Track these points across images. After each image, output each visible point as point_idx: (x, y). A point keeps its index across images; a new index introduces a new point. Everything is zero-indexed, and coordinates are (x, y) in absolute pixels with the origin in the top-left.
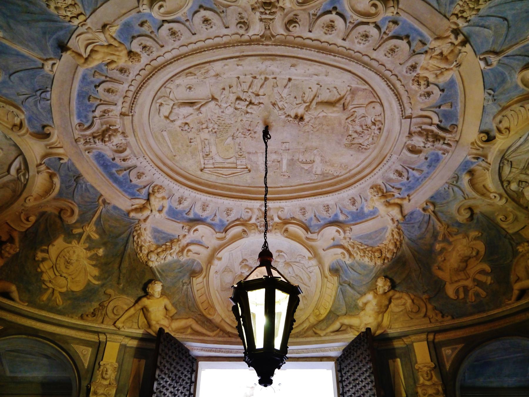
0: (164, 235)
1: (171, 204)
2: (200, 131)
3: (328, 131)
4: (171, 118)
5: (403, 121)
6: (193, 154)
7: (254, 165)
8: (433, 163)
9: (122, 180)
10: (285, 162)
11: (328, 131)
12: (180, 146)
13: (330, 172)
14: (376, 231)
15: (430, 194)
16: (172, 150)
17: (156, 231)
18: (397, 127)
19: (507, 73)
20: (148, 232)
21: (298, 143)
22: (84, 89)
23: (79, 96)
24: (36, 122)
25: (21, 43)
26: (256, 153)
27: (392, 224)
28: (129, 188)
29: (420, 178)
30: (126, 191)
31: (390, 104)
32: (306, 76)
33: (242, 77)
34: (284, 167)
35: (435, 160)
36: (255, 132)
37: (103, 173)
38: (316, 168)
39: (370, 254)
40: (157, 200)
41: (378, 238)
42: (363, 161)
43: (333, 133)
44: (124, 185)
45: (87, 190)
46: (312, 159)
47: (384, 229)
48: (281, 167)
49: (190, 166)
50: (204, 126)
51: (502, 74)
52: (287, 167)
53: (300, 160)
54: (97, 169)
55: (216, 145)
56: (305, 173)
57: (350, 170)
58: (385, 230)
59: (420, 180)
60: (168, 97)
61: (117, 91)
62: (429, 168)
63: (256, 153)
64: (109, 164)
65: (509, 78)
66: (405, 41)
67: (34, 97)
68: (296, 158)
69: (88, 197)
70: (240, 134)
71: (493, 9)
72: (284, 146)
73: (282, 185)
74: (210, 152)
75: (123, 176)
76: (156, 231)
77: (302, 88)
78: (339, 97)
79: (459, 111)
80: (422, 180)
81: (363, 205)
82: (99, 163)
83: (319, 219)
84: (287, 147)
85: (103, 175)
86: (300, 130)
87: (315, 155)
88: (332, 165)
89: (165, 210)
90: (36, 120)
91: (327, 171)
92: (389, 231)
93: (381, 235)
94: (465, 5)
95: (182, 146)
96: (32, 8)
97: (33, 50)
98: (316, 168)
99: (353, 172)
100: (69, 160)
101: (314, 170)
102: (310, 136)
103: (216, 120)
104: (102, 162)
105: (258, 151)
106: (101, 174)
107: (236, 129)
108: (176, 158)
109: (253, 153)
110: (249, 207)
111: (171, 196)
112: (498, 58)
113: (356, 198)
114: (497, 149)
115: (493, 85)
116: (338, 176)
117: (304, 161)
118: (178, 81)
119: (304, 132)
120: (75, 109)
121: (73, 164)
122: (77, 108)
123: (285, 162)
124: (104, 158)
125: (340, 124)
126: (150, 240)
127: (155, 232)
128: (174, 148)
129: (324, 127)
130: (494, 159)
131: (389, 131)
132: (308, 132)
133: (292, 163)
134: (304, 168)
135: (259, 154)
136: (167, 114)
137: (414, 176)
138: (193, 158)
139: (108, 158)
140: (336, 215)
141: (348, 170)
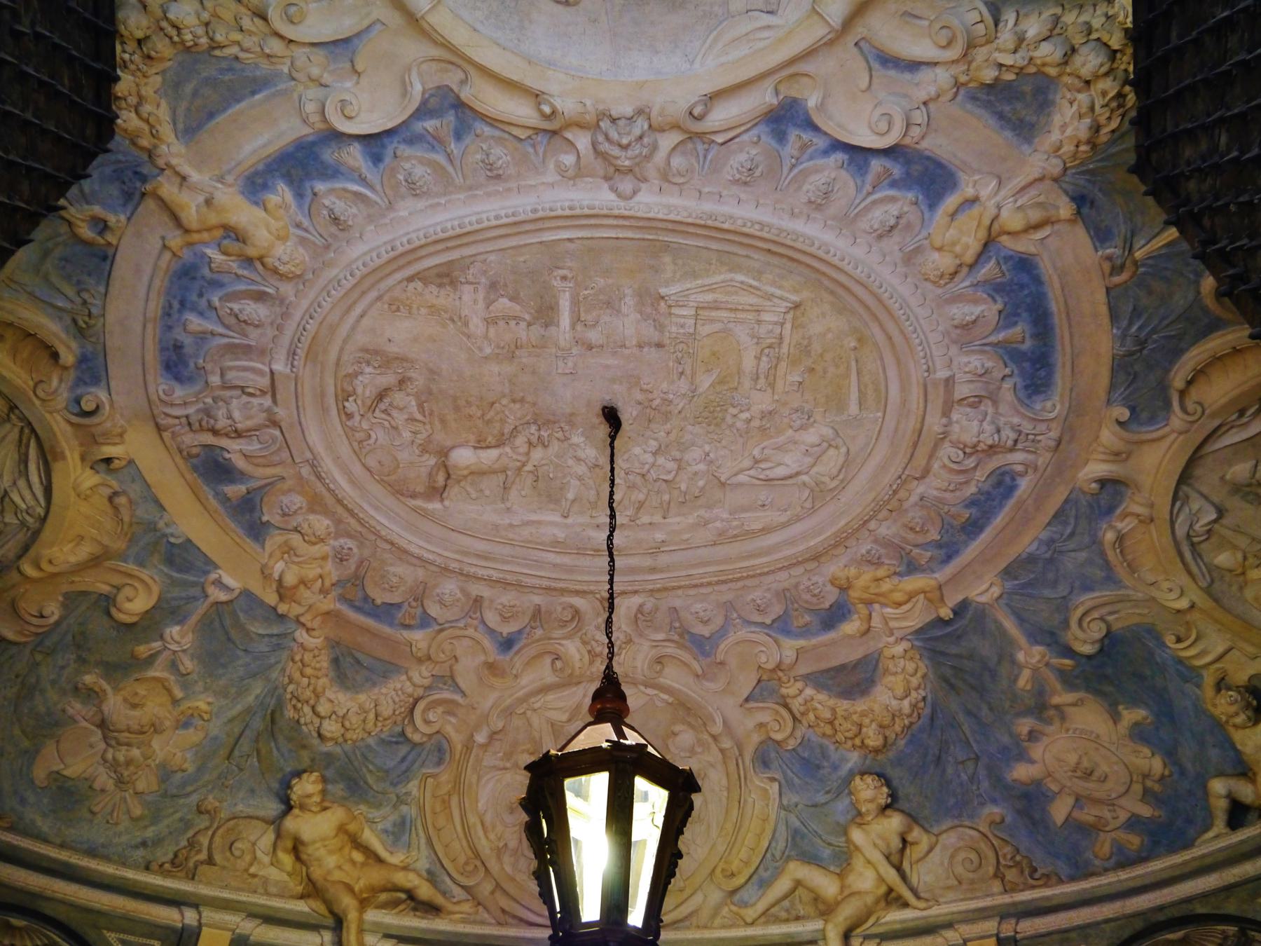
0: (1007, 108)
1: (927, 215)
2: (770, 413)
3: (467, 402)
4: (825, 445)
5: (309, 455)
6: (806, 350)
7: (649, 310)
8: (174, 358)
9: (1025, 315)
10: (565, 320)
11: (467, 402)
12: (832, 370)
13: (433, 288)
14: (211, 115)
15: (122, 268)
16: (853, 363)
17: (1025, 130)
18: (314, 437)
19: (175, 575)
20: (1055, 136)
21: (534, 372)
22: (963, 537)
23: (981, 529)
24: (1102, 502)
25: (1003, 633)
26: (640, 346)
27: (174, 161)
28: (1022, 287)
29: (180, 311)
30: (1038, 281)
31: (353, 481)
32: (533, 522)
33: (657, 518)
34: (565, 304)
35: (176, 366)
36: (640, 404)
37: (1059, 348)
38: (475, 301)
39: (188, 37)
40: (958, 249)
41: (189, 88)
42: (353, 328)
43: (455, 399)
44: (1028, 300)
45: (1136, 313)
46: (492, 331)
47: (189, 132)
48: (575, 303)
49: (824, 315)
50: (756, 423)
51: (180, 571)
52: (557, 304)
53: (523, 325)
54: (1064, 366)
55: (740, 372)
56: (506, 285)
57: (379, 298)
58: (181, 126)
59: (176, 305)
60: (812, 491)
61: (906, 526)
62: (176, 340)
63: (640, 346)
64: (1027, 365)
65: (166, 570)
66: (379, 602)
67: (1064, 548)
68: (537, 330)
69: (1150, 293)
70: (675, 402)
71: (273, 660)
72: (570, 364)
73: (569, 244)
74: (758, 358)
75: (1015, 324)
76: (1025, 130)
77: (539, 495)
78: (462, 484)
79: (205, 488)
80: (171, 306)
81: (300, 206)
82: (1050, 374)
83: (431, 139)
84: (561, 364)
85: (1063, 345)
86: (534, 404)
87: (486, 337)
88: (434, 310)
89: (951, 202)
90: (1099, 507)
91: (443, 292)
92: (166, 131)
93: (183, 106)
94: (318, 666)
95: (825, 372)
96: (949, 673)
97: (996, 621)
98: (475, 301)
99: (373, 294)
100: (1109, 402)
101: (481, 295)
102: (507, 391)
103: (727, 432)
104: (1042, 373)
105: (635, 350)
106: (1063, 349)
107: (683, 414)
108: (853, 344)
109: (650, 345)
110: (676, 188)
111: (909, 258)
112: (211, 599)
113: (333, 229)
114: (68, 453)
115: (183, 558)
116: (410, 279)
117: (513, 323)
118: (783, 519)
119: (522, 400)
120: (1007, 509)
121: (1112, 387)
122: (1001, 506)
123: (565, 320)
124: (1028, 382)
125: (443, 421)
126: (1065, 103)
127: (1032, 126)
128: (848, 368)
129: (479, 413)
130: (55, 435)
131: (325, 410)
132: (514, 401)
133: (546, 313)
134: (511, 299)
135: (634, 343)
136: (832, 452)
137: (201, 314)
138: (810, 338)
139: (1017, 379)
140: (377, 159)
141: (386, 298)
